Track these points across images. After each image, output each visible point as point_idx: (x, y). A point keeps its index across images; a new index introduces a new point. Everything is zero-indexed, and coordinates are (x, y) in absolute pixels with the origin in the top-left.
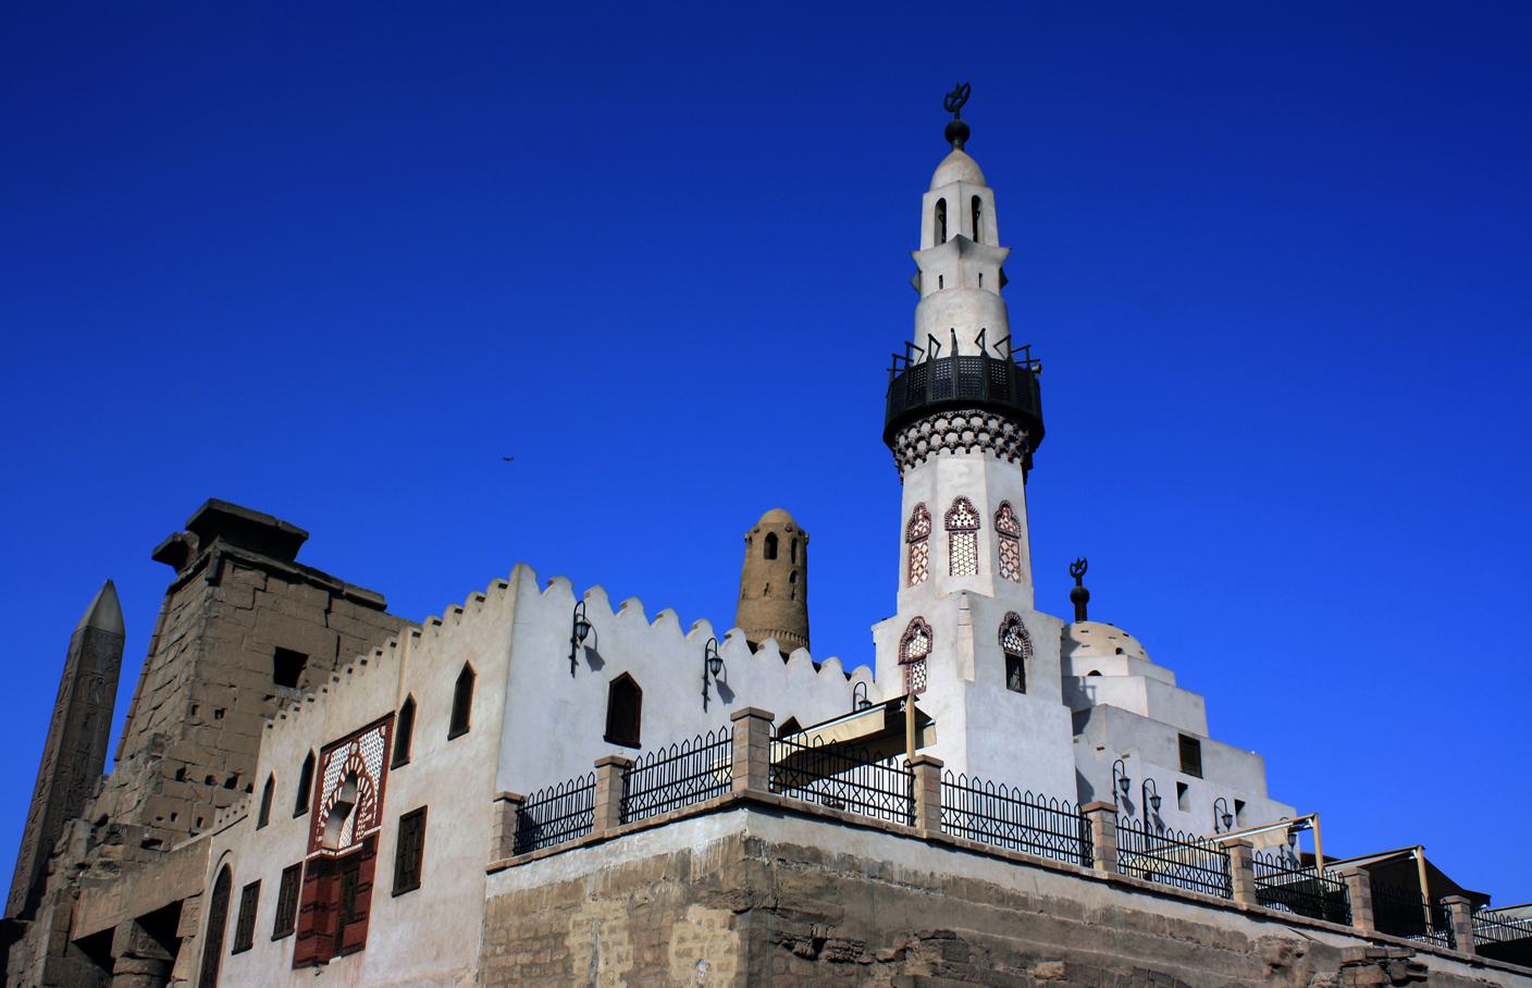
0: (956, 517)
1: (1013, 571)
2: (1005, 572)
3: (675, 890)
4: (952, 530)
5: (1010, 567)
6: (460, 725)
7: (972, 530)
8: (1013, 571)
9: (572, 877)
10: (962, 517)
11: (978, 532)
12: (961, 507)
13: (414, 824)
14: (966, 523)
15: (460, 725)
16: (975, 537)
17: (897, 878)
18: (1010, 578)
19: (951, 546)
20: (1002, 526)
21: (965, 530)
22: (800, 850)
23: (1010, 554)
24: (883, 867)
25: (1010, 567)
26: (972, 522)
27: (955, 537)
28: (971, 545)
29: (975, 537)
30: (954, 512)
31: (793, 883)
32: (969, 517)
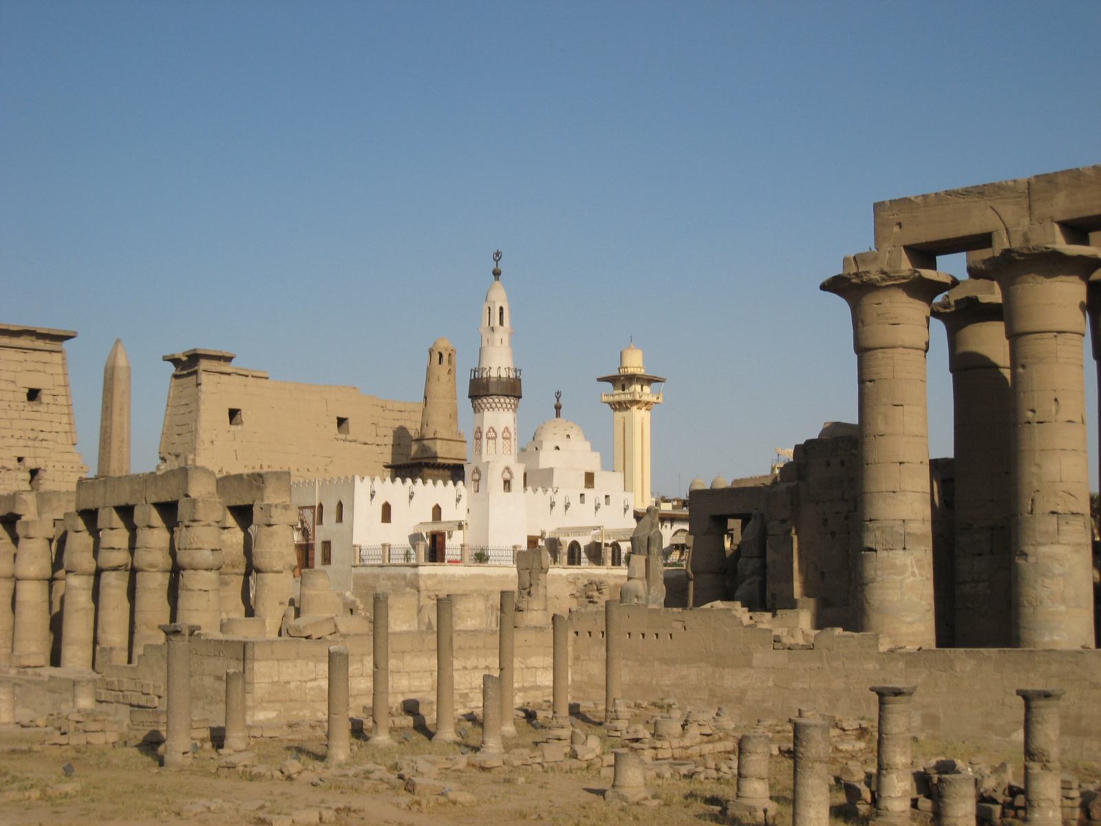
3: (403, 583)
4: (488, 438)
6: (340, 519)
7: (495, 438)
9: (377, 573)
13: (327, 545)
15: (340, 519)
21: (492, 438)
22: (432, 575)
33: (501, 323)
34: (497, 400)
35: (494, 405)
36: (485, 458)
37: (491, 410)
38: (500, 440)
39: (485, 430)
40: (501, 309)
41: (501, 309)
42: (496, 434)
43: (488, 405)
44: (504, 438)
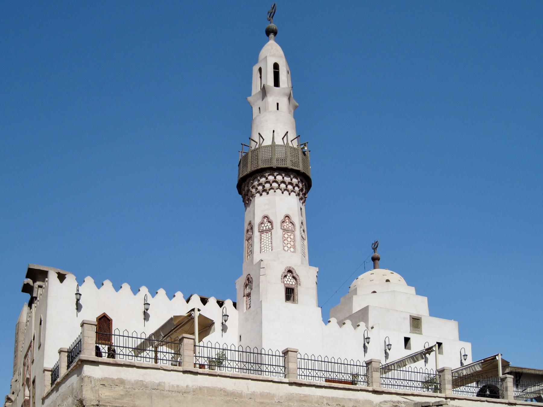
0: (263, 225)
1: (290, 248)
2: (286, 248)
4: (262, 232)
5: (289, 246)
8: (290, 248)
10: (266, 225)
11: (273, 231)
12: (265, 220)
14: (267, 227)
16: (271, 234)
17: (167, 388)
18: (289, 251)
19: (261, 240)
20: (285, 227)
21: (267, 231)
22: (113, 380)
23: (289, 239)
24: (159, 384)
25: (289, 246)
26: (270, 227)
27: (263, 235)
28: (270, 238)
29: (271, 234)
30: (262, 223)
31: (107, 394)
32: (269, 224)
33: (277, 83)
34: (271, 178)
35: (267, 186)
36: (257, 257)
37: (264, 194)
38: (278, 232)
39: (257, 221)
40: (276, 66)
41: (276, 66)
42: (272, 227)
43: (260, 188)
44: (285, 230)
